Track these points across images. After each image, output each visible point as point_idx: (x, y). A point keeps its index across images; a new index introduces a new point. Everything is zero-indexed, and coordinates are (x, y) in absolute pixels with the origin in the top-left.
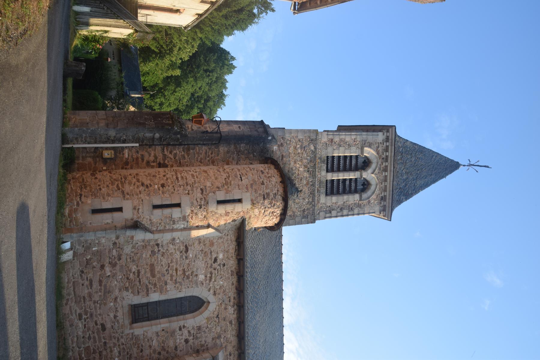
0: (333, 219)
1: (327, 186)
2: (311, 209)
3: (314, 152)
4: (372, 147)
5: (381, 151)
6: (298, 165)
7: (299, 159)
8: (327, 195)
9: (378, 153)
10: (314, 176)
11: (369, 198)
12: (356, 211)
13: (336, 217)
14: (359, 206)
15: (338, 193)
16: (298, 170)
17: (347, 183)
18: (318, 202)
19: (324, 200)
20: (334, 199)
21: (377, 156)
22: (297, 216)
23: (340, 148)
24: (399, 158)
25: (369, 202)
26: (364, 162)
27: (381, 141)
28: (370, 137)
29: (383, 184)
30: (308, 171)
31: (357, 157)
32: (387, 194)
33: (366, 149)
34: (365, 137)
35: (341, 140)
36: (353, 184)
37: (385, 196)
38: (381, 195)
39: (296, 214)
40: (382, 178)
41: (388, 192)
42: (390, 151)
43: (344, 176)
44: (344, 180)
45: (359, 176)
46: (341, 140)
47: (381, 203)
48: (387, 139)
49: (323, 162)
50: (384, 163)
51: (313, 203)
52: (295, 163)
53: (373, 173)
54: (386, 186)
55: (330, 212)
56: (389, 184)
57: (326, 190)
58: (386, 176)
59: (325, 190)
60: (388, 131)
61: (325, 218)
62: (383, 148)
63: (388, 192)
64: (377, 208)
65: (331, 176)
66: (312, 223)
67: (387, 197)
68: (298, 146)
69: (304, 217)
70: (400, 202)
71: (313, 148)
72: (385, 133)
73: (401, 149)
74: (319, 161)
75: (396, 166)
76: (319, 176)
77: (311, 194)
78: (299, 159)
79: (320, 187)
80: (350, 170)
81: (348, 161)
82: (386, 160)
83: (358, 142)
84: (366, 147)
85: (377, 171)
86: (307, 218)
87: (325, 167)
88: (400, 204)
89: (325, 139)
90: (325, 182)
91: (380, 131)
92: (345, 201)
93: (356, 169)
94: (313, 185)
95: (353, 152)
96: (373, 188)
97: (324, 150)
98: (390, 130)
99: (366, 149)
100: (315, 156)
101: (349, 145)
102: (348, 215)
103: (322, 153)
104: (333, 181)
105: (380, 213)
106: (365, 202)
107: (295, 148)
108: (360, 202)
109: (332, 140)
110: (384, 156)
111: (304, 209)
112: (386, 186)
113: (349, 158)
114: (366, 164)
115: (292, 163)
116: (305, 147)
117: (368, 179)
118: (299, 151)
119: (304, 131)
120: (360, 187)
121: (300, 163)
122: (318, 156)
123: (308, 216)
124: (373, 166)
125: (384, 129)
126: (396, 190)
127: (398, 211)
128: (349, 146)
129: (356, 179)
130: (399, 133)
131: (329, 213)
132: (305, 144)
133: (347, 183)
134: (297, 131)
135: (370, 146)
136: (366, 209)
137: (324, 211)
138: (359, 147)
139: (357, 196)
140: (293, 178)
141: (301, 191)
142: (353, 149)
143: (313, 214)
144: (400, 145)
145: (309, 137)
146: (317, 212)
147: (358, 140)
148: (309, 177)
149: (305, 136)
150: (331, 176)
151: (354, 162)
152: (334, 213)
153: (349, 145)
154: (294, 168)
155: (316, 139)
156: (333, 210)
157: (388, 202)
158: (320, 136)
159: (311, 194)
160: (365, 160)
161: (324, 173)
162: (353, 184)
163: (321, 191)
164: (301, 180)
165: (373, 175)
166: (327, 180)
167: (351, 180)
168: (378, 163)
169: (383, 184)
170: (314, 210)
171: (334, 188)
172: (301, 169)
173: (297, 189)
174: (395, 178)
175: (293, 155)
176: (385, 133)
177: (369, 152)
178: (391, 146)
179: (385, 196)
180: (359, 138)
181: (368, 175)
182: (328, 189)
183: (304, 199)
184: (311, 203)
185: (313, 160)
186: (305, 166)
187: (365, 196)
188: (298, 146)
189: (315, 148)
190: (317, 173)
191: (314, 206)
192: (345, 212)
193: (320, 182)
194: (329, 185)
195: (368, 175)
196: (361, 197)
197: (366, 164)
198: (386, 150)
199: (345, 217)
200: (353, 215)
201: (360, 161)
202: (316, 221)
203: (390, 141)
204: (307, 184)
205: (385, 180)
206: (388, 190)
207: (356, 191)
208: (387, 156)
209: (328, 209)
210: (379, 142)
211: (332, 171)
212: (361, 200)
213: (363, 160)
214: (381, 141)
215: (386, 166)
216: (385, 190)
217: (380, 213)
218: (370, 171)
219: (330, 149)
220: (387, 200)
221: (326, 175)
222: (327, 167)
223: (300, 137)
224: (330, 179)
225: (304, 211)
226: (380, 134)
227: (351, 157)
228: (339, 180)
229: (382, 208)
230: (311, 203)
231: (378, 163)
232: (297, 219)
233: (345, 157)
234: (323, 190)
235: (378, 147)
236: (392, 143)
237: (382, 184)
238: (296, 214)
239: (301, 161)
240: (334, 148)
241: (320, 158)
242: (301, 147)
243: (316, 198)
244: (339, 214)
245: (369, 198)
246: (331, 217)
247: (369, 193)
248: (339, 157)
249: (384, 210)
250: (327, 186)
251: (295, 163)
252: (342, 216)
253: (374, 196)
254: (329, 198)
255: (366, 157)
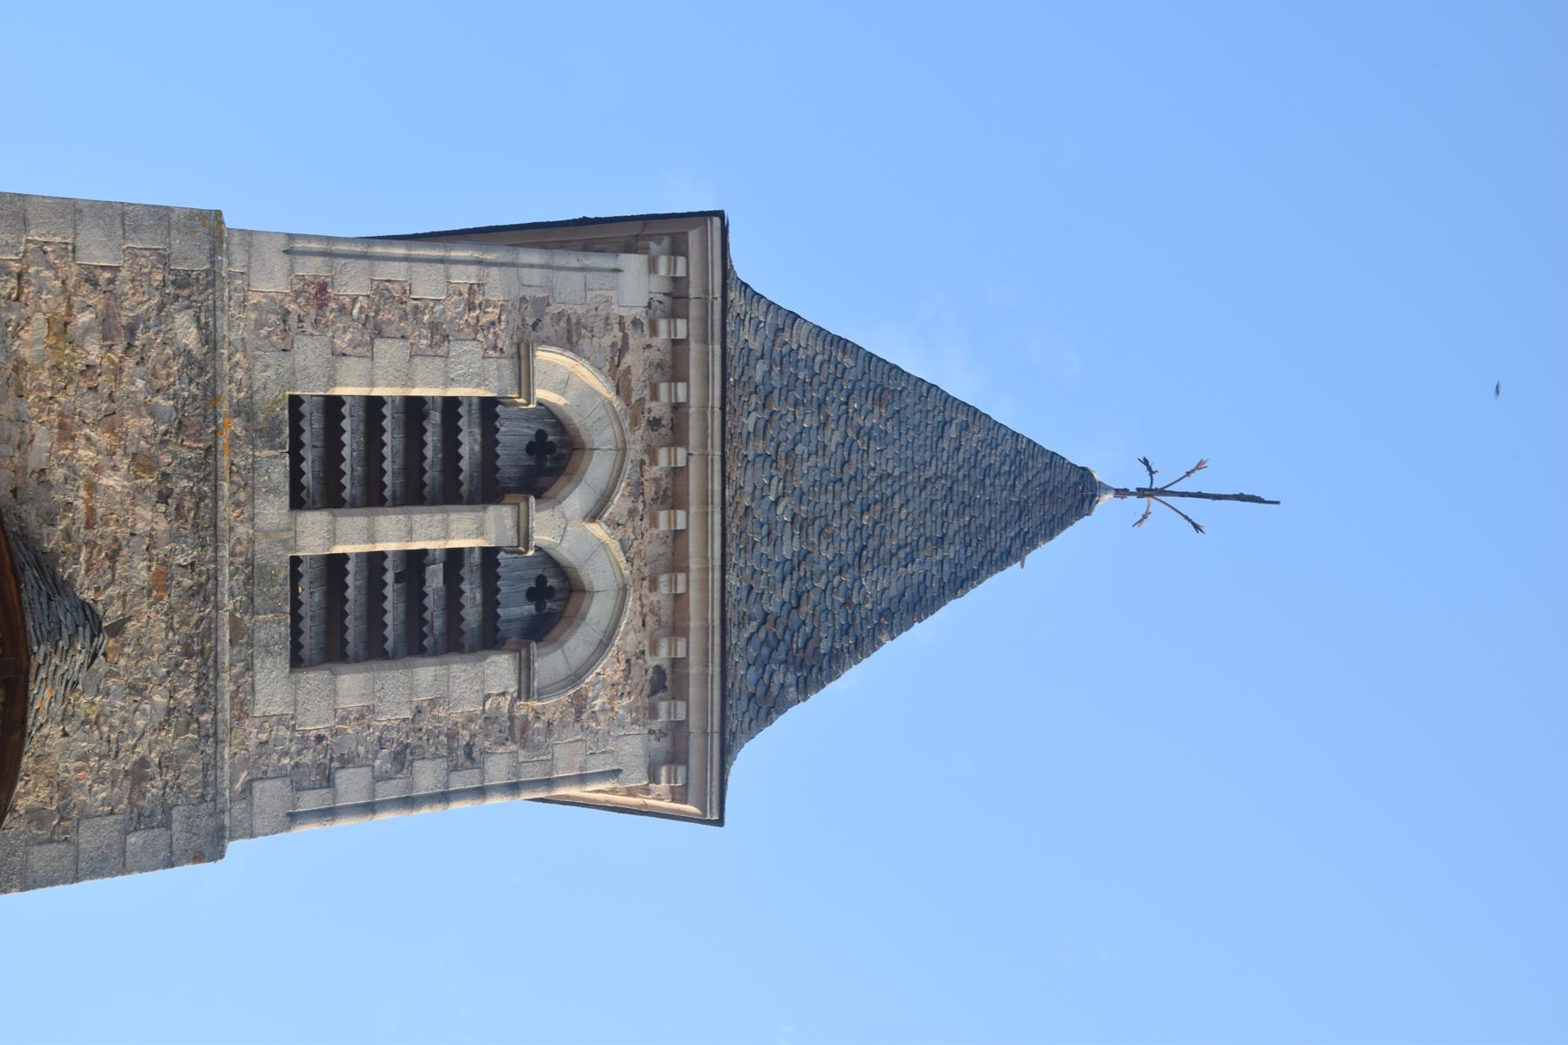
0: (346, 826)
1: (296, 604)
2: (194, 762)
3: (202, 365)
4: (585, 344)
5: (638, 372)
6: (85, 454)
7: (90, 407)
8: (297, 662)
9: (622, 389)
10: (208, 532)
11: (577, 677)
12: (498, 768)
13: (370, 808)
14: (517, 732)
15: (375, 651)
16: (92, 487)
17: (435, 579)
18: (242, 710)
19: (285, 699)
20: (352, 685)
21: (618, 404)
22: (85, 815)
23: (381, 345)
24: (750, 423)
25: (580, 705)
26: (538, 446)
27: (639, 313)
28: (571, 283)
29: (664, 589)
30: (164, 498)
31: (488, 406)
32: (691, 647)
33: (546, 357)
34: (534, 277)
35: (382, 293)
36: (471, 592)
37: (675, 662)
38: (652, 662)
39: (79, 797)
40: (652, 548)
41: (694, 637)
42: (694, 373)
43: (410, 534)
44: (415, 562)
45: (509, 538)
46: (382, 293)
47: (653, 712)
48: (676, 299)
49: (268, 435)
50: (663, 454)
51: (202, 720)
52: (65, 433)
53: (594, 516)
54: (679, 600)
55: (328, 781)
56: (697, 586)
57: (296, 632)
58: (678, 536)
59: (285, 630)
60: (678, 249)
61: (294, 818)
62: (655, 356)
63: (694, 637)
64: (632, 747)
65: (317, 534)
66: (199, 858)
67: (694, 670)
68: (85, 318)
69: (139, 820)
70: (767, 707)
71: (189, 337)
72: (663, 262)
73: (761, 367)
74: (237, 426)
75: (735, 475)
76: (242, 530)
77: (188, 653)
78: (90, 407)
79: (250, 606)
80: (450, 494)
81: (432, 437)
82: (677, 437)
83: (493, 313)
84: (547, 342)
85: (619, 504)
86: (167, 824)
87: (279, 472)
88: (768, 721)
89: (271, 281)
90: (285, 573)
91: (630, 248)
92: (423, 697)
93: (489, 491)
94: (203, 592)
95: (466, 377)
96: (598, 611)
97: (271, 358)
98: (693, 237)
99: (546, 357)
100: (211, 395)
101: (434, 327)
102: (445, 797)
103: (260, 377)
104: (335, 565)
105: (653, 777)
106: (553, 705)
107: (61, 329)
108: (525, 708)
109: (322, 288)
110: (659, 408)
111: (143, 762)
112: (679, 600)
113: (436, 417)
114: (551, 456)
115: (43, 439)
116: (131, 330)
117: (568, 551)
118: (93, 351)
119: (121, 217)
120: (515, 609)
121: (103, 439)
122: (230, 393)
123: (168, 810)
124: (597, 469)
125: (658, 238)
126: (741, 625)
127: (756, 760)
128: (440, 334)
129: (489, 554)
130: (743, 268)
131: (318, 783)
132: (136, 303)
133: (435, 579)
134: (72, 211)
135: (569, 341)
136: (566, 755)
137: (281, 774)
138: (504, 342)
139: (500, 669)
140: (52, 540)
141: (117, 629)
142: (466, 353)
143: (209, 792)
144: (755, 345)
145: (164, 259)
146: (231, 780)
147: (496, 296)
148: (174, 537)
149: (133, 253)
150: (317, 534)
151: (469, 443)
152: (352, 784)
153: (434, 327)
154: (60, 473)
155: (212, 278)
156: (345, 762)
157: (697, 705)
158: (239, 256)
159: (188, 653)
160: (541, 434)
161: (273, 511)
162: (471, 592)
163: (261, 635)
164: (113, 557)
165: (598, 530)
166: (296, 561)
167: (454, 558)
168: (623, 451)
169: (664, 589)
170: (210, 765)
171: (346, 619)
172: (112, 481)
173: (89, 617)
174: (732, 549)
175: (44, 377)
176: (663, 262)
177: (566, 380)
178: (705, 340)
179: (675, 662)
180: (497, 287)
181: (565, 528)
182: (306, 625)
183: (136, 690)
184: (191, 718)
185: (197, 416)
186: (142, 463)
187: (550, 663)
188: (85, 318)
189: (210, 339)
190: (227, 512)
191: (212, 736)
192: (427, 776)
193: (253, 573)
194: (312, 596)
195: (565, 528)
196: (525, 670)
197: (551, 456)
198: (674, 367)
199: (425, 812)
200: (481, 792)
201: (513, 435)
202: (233, 847)
203: (694, 310)
204: (162, 580)
205: (677, 564)
206: (694, 623)
207: (490, 639)
208: (678, 408)
209: (307, 757)
210: (629, 315)
211: (332, 499)
212: (526, 690)
213: (528, 431)
214: (639, 313)
215: (677, 473)
216: (677, 629)
217: (653, 777)
218: (576, 500)
219: (309, 352)
220: (694, 691)
221: (292, 528)
222: (295, 473)
223: (97, 251)
224: (321, 552)
225: (139, 773)
226: (633, 263)
227: (451, 404)
228: (375, 561)
229: (664, 744)
230: (191, 718)
231: (623, 451)
232: (89, 838)
233: (414, 408)
234: (273, 628)
235: (621, 349)
236: (705, 320)
237: (654, 586)
238: (79, 797)
239: (110, 420)
240: (342, 343)
241: (245, 411)
242: (106, 328)
243: (227, 686)
244: (388, 790)
245: (577, 677)
246: (329, 813)
247: (578, 643)
248: (373, 405)
249: (676, 757)
250: (296, 604)
251: (65, 433)
252: (409, 802)
253: (609, 668)
254: (313, 679)
255: (546, 410)
